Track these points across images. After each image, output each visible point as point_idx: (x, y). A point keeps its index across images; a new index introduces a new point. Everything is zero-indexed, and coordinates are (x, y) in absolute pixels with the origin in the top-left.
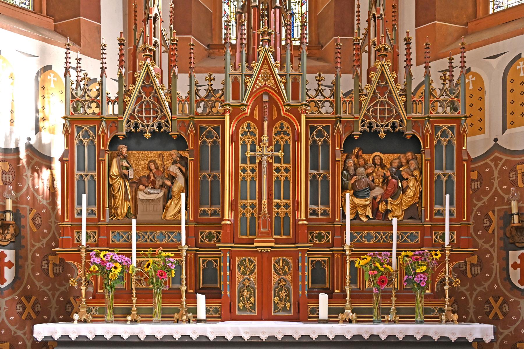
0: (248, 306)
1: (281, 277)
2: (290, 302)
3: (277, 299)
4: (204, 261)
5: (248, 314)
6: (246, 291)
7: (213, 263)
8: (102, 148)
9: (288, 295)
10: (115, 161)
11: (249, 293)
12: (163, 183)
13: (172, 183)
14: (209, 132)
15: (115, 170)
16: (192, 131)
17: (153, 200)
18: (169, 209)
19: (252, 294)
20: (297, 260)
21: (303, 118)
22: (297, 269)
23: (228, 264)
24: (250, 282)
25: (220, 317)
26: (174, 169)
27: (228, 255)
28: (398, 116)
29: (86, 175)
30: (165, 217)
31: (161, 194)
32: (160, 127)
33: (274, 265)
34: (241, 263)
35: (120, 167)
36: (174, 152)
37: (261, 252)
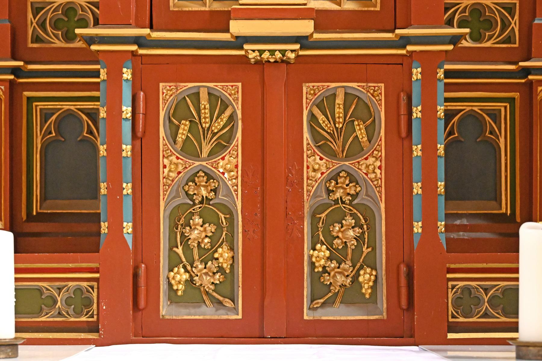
0: (206, 282)
1: (337, 165)
2: (374, 268)
3: (323, 252)
4: (46, 115)
5: (207, 312)
6: (198, 220)
7: (81, 120)
9: (366, 238)
11: (210, 228)
19: (223, 235)
20: (403, 96)
23: (127, 110)
24: (213, 184)
25: (93, 328)
27: (127, 74)
33: (313, 117)
34: (179, 111)
37: (259, 63)
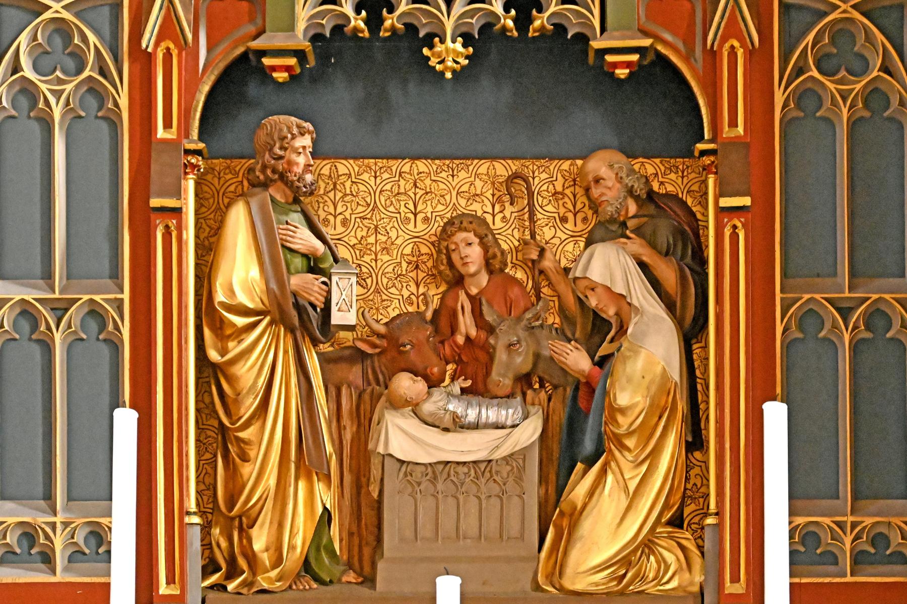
8: (161, 133)
10: (238, 220)
12: (537, 357)
13: (602, 362)
14: (841, 32)
15: (241, 274)
16: (732, 29)
17: (482, 468)
18: (586, 526)
26: (611, 268)
29: (60, 309)
30: (558, 568)
31: (529, 432)
35: (274, 254)
36: (602, 165)
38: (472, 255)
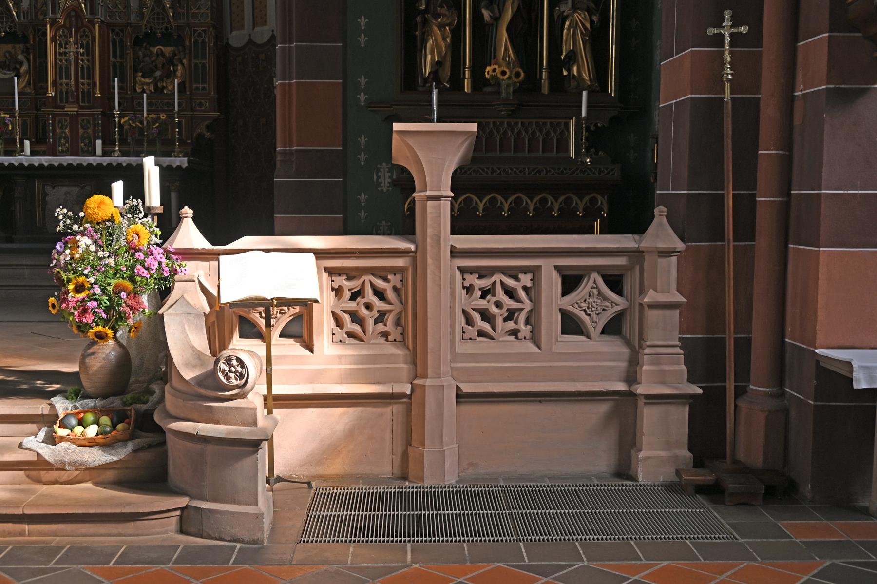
21: (97, 26)
22: (95, 125)
26: (21, 57)
28: (169, 22)
32: (10, 28)
34: (60, 122)
38: (7, 55)
